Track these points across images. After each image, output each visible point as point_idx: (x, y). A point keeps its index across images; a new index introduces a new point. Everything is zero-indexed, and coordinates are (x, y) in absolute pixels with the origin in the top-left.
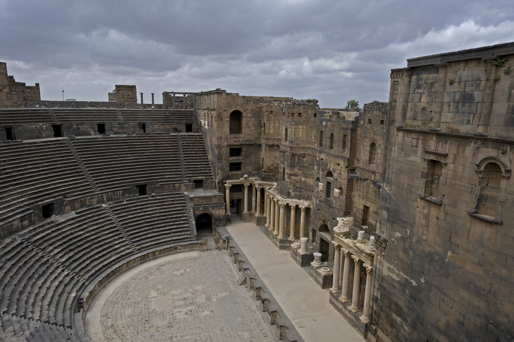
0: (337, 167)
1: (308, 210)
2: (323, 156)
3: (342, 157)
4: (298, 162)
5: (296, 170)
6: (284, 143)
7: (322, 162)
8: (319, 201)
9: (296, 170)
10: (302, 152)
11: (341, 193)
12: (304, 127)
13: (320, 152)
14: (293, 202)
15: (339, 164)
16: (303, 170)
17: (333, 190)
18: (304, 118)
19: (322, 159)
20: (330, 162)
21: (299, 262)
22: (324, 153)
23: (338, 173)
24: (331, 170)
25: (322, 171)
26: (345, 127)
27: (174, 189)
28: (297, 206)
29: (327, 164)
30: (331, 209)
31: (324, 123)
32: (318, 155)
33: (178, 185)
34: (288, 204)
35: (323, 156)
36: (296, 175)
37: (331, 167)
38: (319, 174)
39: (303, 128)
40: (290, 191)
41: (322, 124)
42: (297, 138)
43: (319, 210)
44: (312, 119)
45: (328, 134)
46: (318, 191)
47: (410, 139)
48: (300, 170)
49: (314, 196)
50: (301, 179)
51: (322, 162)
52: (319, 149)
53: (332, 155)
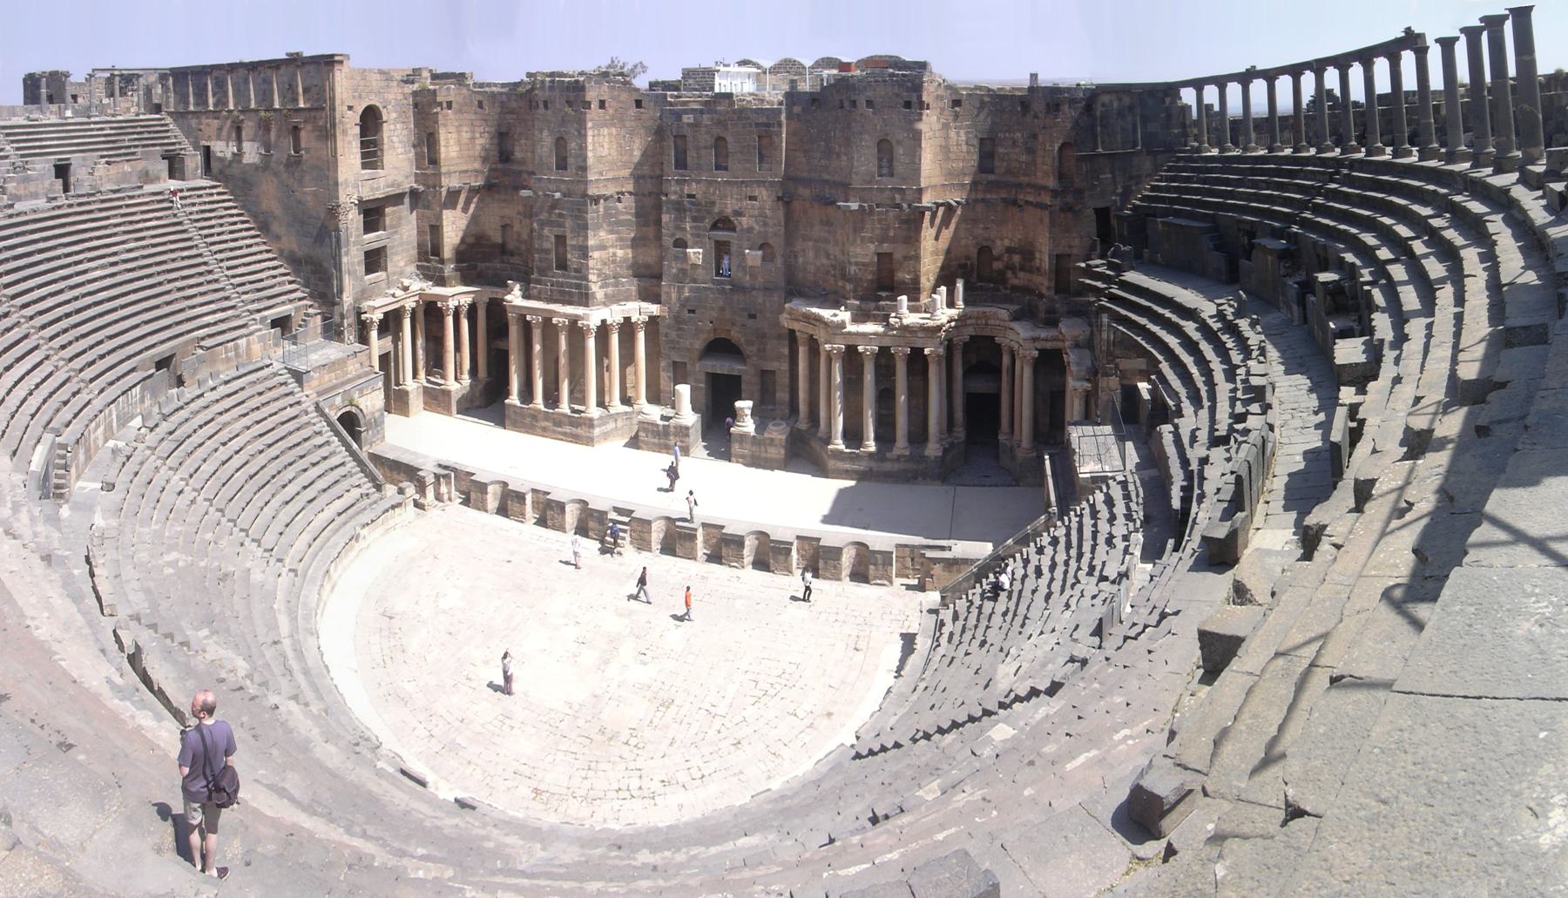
1: (652, 323)
2: (693, 188)
4: (607, 215)
5: (602, 234)
8: (691, 290)
9: (602, 234)
10: (611, 190)
12: (614, 131)
14: (614, 314)
16: (617, 232)
18: (611, 111)
19: (693, 196)
25: (695, 219)
27: (237, 355)
28: (627, 319)
29: (713, 203)
33: (242, 342)
34: (604, 321)
36: (602, 247)
37: (730, 205)
39: (610, 135)
40: (594, 288)
42: (599, 159)
43: (691, 311)
44: (633, 111)
48: (611, 232)
50: (614, 254)
52: (672, 175)
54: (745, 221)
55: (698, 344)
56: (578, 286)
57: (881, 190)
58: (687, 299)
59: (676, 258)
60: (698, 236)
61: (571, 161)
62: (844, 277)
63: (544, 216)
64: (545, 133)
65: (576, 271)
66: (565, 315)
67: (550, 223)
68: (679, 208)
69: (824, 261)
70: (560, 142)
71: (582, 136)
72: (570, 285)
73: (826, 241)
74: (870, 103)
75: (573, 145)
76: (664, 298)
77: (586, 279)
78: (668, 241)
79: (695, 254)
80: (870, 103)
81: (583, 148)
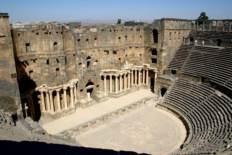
0: (93, 53)
2: (83, 51)
3: (96, 48)
6: (54, 53)
7: (83, 54)
13: (80, 50)
15: (94, 51)
17: (92, 63)
19: (82, 53)
21: (91, 105)
22: (84, 49)
24: (90, 55)
25: (83, 58)
26: (95, 34)
30: (93, 72)
31: (80, 35)
32: (78, 51)
35: (83, 51)
37: (89, 54)
38: (81, 61)
41: (79, 35)
43: (83, 78)
46: (81, 70)
47: (167, 31)
49: (79, 74)
51: (83, 54)
53: (89, 49)
57: (119, 46)
58: (83, 76)
59: (80, 67)
61: (59, 48)
62: (112, 64)
63: (53, 64)
67: (54, 66)
68: (80, 57)
73: (106, 58)
75: (59, 44)
76: (78, 77)
80: (117, 30)
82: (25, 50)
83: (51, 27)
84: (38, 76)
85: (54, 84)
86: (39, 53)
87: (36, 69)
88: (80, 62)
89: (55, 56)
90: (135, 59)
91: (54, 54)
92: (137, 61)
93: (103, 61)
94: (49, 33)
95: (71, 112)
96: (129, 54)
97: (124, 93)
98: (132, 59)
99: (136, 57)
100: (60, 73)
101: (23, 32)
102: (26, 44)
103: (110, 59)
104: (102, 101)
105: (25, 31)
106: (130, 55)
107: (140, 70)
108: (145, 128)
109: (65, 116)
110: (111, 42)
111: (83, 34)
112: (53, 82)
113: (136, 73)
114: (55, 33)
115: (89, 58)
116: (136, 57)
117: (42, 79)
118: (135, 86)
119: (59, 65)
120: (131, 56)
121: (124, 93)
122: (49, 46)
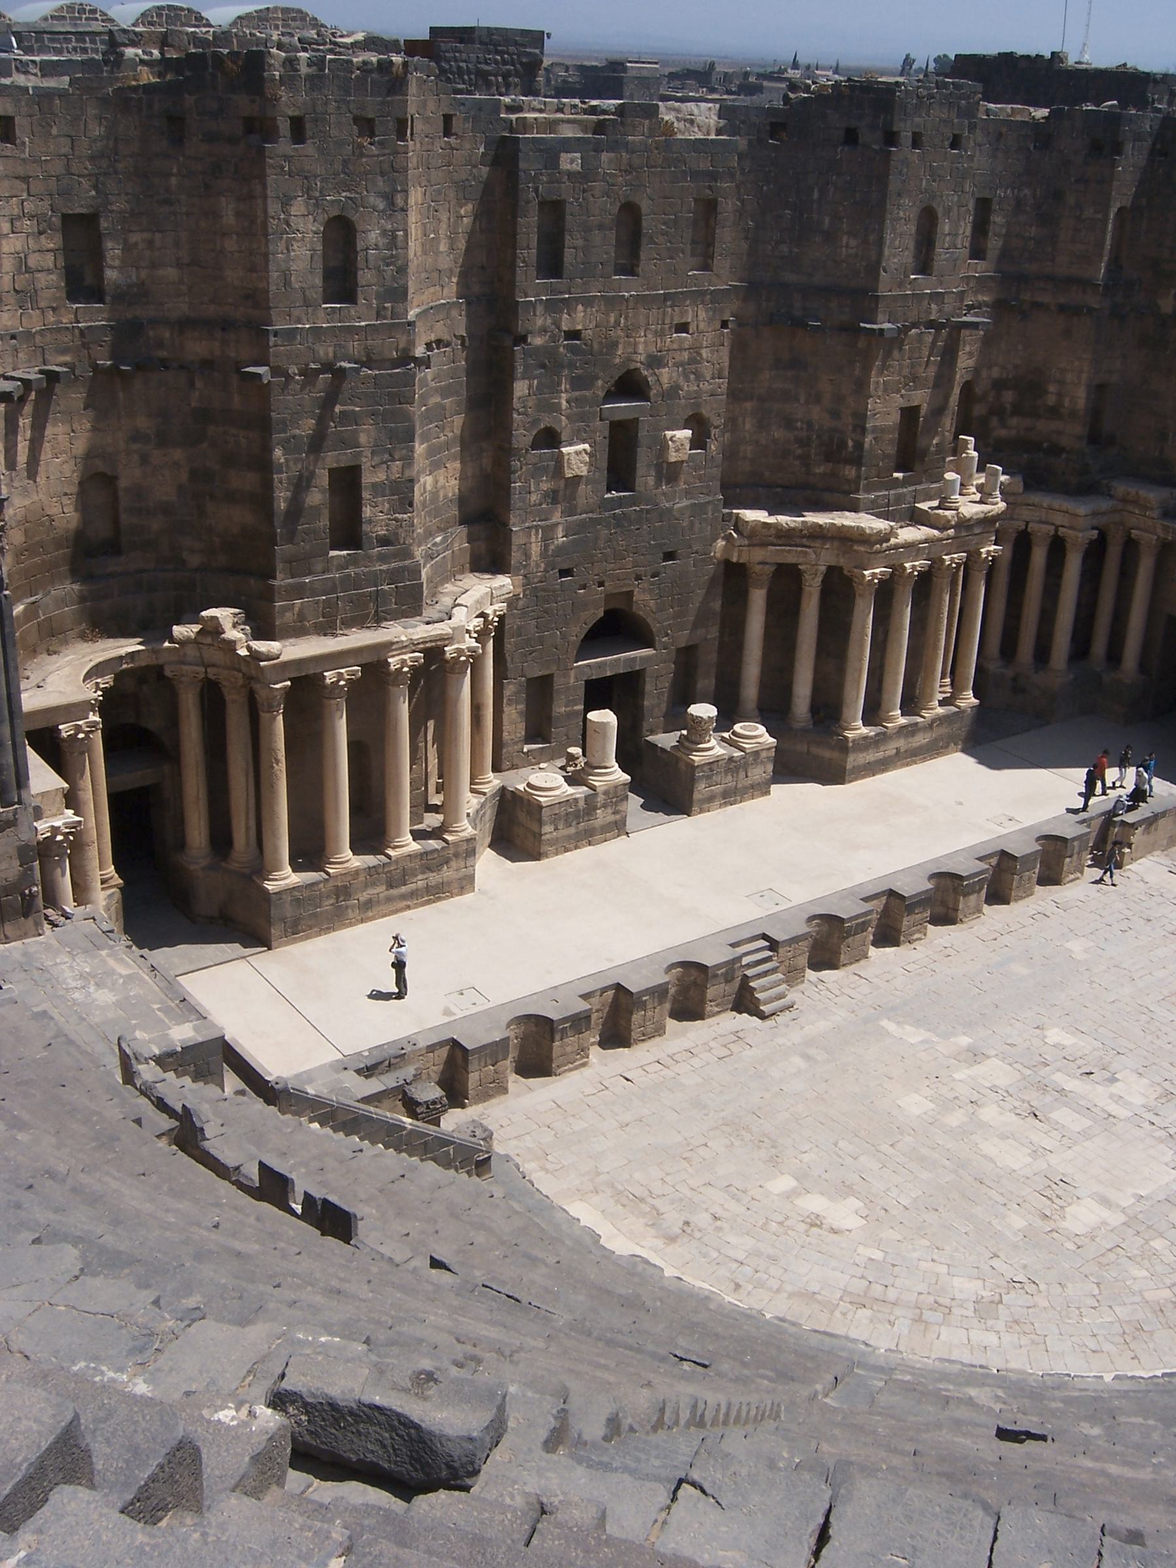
2: (579, 318)
3: (698, 296)
11: (698, 442)
15: (683, 328)
20: (629, 332)
22: (588, 302)
23: (682, 364)
25: (578, 383)
31: (570, 162)
38: (557, 408)
41: (553, 162)
45: (604, 208)
54: (666, 375)
55: (577, 632)
56: (394, 576)
58: (561, 550)
59: (538, 471)
60: (582, 417)
61: (365, 277)
64: (298, 207)
65: (384, 541)
66: (413, 646)
69: (778, 433)
70: (341, 234)
71: (395, 208)
72: (375, 579)
74: (916, 142)
75: (374, 236)
76: (516, 557)
77: (407, 554)
78: (522, 436)
79: (577, 455)
80: (916, 142)
81: (394, 242)
82: (54, 277)
83: (304, 70)
84: (156, 524)
85: (301, 617)
86: (180, 307)
87: (144, 460)
88: (546, 422)
89: (326, 351)
90: (1044, 426)
91: (316, 331)
92: (1056, 450)
93: (748, 425)
94: (284, 127)
95: (434, 878)
96: (996, 372)
97: (921, 739)
98: (1014, 421)
99: (1054, 412)
100: (367, 512)
101: (44, 97)
102: (65, 218)
103: (817, 413)
104: (711, 799)
105: (62, 94)
106: (999, 385)
107: (1080, 538)
108: (1117, 1088)
109: (384, 908)
110: (848, 245)
111: (598, 149)
112: (299, 591)
113: (1039, 557)
114: (340, 128)
115: (630, 386)
116: (1054, 412)
117: (195, 560)
118: (1015, 679)
119: (363, 439)
120: (1009, 396)
121: (921, 739)
122: (281, 246)
